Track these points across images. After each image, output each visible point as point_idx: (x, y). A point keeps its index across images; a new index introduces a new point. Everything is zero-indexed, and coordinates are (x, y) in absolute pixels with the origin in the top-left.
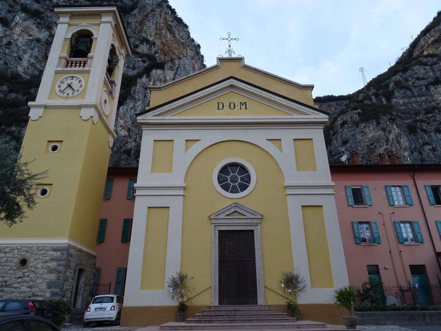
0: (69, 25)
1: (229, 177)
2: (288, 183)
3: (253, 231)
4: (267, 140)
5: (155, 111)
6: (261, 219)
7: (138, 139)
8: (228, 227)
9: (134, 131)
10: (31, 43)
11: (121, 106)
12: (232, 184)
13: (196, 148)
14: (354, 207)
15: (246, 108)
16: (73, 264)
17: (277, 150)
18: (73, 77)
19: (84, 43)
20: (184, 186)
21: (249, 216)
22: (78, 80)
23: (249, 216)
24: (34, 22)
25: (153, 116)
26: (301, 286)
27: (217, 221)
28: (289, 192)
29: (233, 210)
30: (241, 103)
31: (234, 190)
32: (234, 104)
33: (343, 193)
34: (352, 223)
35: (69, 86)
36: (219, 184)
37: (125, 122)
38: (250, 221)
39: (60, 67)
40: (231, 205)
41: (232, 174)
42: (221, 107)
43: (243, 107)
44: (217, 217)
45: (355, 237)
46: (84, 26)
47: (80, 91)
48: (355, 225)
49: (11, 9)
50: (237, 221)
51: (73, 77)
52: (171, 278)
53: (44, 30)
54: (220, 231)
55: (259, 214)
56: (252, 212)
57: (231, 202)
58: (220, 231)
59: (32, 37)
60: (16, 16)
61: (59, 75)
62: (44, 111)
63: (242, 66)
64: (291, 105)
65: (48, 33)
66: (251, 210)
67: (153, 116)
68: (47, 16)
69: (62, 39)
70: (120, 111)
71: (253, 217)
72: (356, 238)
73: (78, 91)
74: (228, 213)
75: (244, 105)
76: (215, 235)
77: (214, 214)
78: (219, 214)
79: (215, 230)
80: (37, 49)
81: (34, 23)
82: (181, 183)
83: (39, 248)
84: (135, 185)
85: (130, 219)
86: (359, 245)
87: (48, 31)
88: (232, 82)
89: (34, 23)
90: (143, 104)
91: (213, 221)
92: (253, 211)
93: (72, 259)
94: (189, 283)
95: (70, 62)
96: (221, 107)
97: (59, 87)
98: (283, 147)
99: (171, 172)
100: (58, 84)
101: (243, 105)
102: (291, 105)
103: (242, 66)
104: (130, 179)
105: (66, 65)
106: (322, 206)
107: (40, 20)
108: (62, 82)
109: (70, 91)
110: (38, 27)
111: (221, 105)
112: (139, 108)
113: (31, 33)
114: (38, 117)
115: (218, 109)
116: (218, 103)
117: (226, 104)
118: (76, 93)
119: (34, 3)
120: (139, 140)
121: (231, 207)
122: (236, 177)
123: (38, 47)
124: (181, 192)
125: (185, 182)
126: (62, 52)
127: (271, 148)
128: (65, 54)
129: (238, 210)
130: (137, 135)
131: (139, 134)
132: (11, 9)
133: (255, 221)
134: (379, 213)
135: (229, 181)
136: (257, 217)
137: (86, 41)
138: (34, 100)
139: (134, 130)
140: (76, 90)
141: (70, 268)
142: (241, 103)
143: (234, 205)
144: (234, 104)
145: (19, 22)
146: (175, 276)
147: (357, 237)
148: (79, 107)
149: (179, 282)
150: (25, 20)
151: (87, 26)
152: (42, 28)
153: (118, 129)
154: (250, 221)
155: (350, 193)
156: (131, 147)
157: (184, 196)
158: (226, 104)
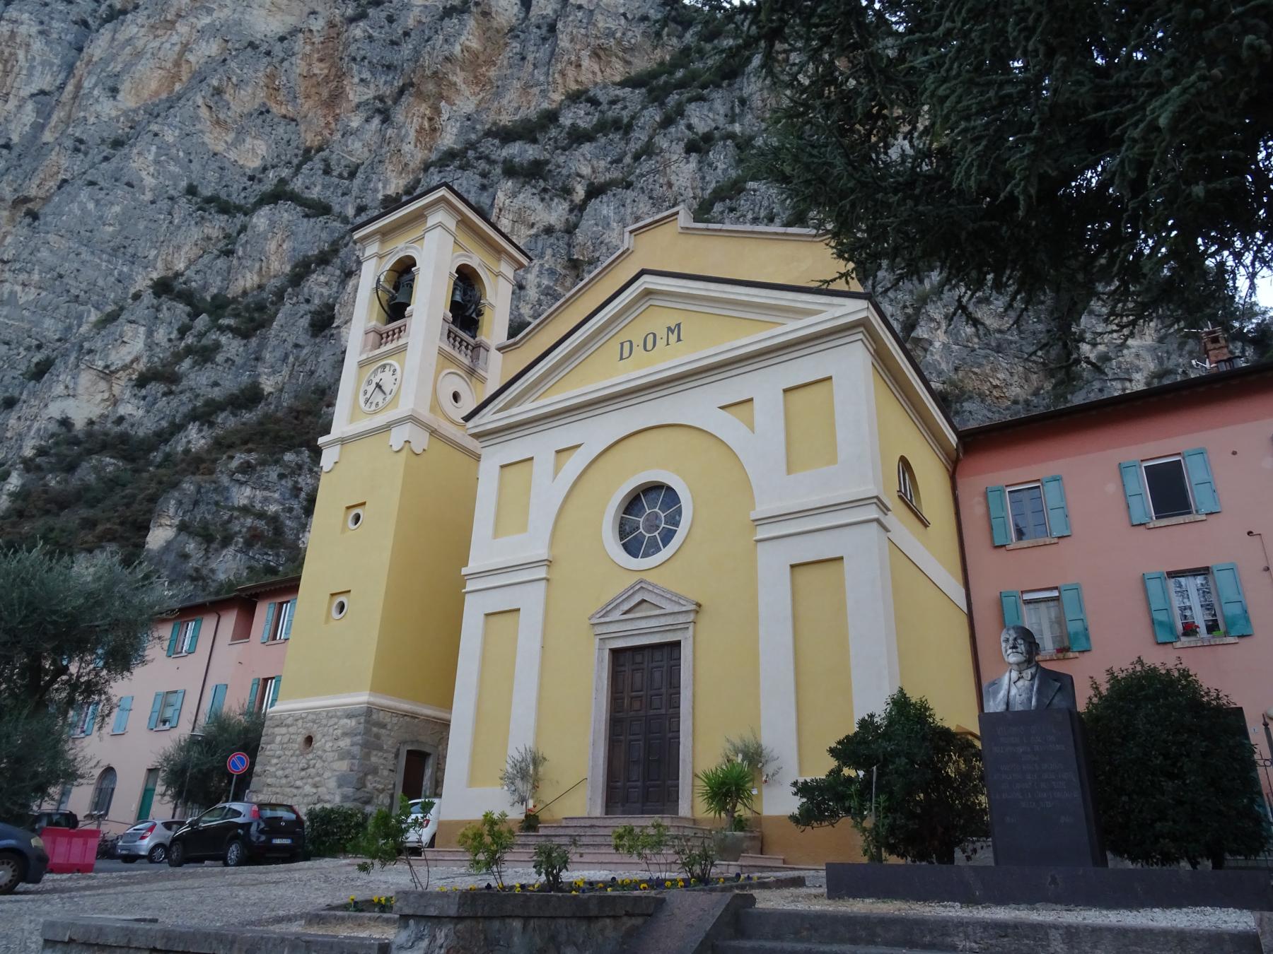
2: (763, 508)
4: (720, 408)
5: (496, 402)
8: (628, 639)
10: (536, 243)
13: (575, 464)
14: (1151, 525)
15: (679, 340)
16: (388, 743)
18: (384, 366)
21: (670, 608)
24: (534, 191)
26: (769, 769)
28: (763, 533)
29: (637, 599)
30: (669, 329)
32: (655, 336)
33: (1112, 488)
34: (1144, 580)
35: (379, 386)
38: (669, 620)
43: (673, 338)
44: (603, 620)
45: (1153, 621)
48: (1154, 586)
49: (485, 181)
50: (643, 624)
51: (384, 366)
53: (556, 200)
56: (675, 598)
58: (615, 653)
59: (536, 227)
60: (496, 193)
62: (342, 448)
63: (680, 230)
64: (776, 298)
65: (566, 205)
66: (671, 593)
68: (559, 166)
71: (677, 609)
72: (1157, 628)
74: (626, 607)
76: (601, 661)
78: (607, 612)
80: (549, 251)
81: (534, 194)
82: (542, 553)
83: (331, 714)
84: (464, 571)
86: (1170, 646)
87: (565, 199)
88: (648, 282)
89: (534, 194)
92: (676, 595)
93: (383, 731)
95: (384, 336)
98: (759, 418)
102: (776, 298)
103: (680, 230)
105: (378, 343)
106: (841, 558)
107: (545, 180)
109: (379, 397)
110: (543, 200)
113: (532, 219)
114: (332, 464)
115: (621, 359)
117: (638, 341)
118: (389, 398)
119: (527, 146)
121: (631, 592)
123: (551, 245)
124: (541, 573)
126: (369, 320)
127: (727, 427)
132: (485, 181)
133: (682, 619)
134: (1250, 533)
136: (684, 609)
141: (380, 748)
142: (669, 329)
143: (638, 587)
145: (504, 204)
147: (1161, 623)
148: (388, 427)
150: (514, 195)
151: (407, 248)
152: (552, 199)
154: (669, 620)
155: (1140, 485)
157: (548, 580)
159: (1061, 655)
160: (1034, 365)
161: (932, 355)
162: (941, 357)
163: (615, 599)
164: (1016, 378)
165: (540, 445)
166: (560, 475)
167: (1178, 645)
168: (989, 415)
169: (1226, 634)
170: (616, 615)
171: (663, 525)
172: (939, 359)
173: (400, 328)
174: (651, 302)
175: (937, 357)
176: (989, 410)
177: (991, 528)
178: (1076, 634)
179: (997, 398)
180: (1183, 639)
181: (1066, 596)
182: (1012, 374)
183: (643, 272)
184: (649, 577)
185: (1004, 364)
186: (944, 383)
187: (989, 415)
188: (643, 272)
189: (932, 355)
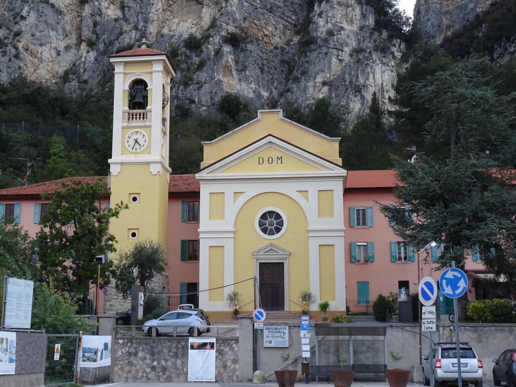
0: (125, 74)
1: (267, 222)
2: (310, 228)
3: (283, 263)
5: (208, 169)
6: (289, 255)
7: (141, 24)
9: (133, 8)
12: (270, 227)
13: (242, 199)
15: (282, 163)
17: (305, 201)
18: (137, 132)
19: (140, 91)
20: (234, 230)
21: (281, 253)
22: (142, 135)
23: (281, 253)
25: (207, 173)
26: (313, 299)
27: (258, 257)
28: (311, 234)
29: (269, 248)
30: (278, 157)
31: (271, 233)
34: (391, 243)
35: (136, 141)
36: (260, 227)
38: (281, 256)
39: (125, 122)
40: (268, 245)
41: (269, 220)
42: (261, 162)
43: (279, 161)
44: (258, 254)
45: (391, 256)
46: (138, 75)
47: (145, 146)
48: (393, 245)
50: (272, 256)
52: (228, 294)
54: (260, 263)
55: (287, 251)
56: (283, 250)
57: (268, 242)
58: (260, 263)
61: (126, 130)
67: (207, 173)
69: (122, 92)
71: (284, 253)
73: (144, 146)
74: (265, 250)
75: (280, 159)
76: (257, 266)
77: (256, 251)
79: (256, 262)
82: (232, 228)
85: (186, 240)
88: (270, 139)
91: (255, 257)
92: (284, 249)
94: (239, 298)
95: (131, 114)
96: (261, 162)
97: (128, 142)
98: (310, 198)
99: (224, 219)
100: (126, 139)
101: (279, 159)
104: (182, 202)
108: (129, 137)
109: (137, 146)
111: (261, 160)
115: (259, 164)
116: (259, 158)
117: (266, 159)
118: (143, 148)
120: (143, 26)
122: (273, 222)
124: (232, 235)
125: (234, 227)
126: (123, 106)
127: (300, 199)
128: (127, 108)
129: (273, 248)
130: (138, 15)
131: (142, 13)
133: (285, 256)
135: (267, 225)
136: (286, 254)
137: (141, 89)
139: (132, 6)
140: (142, 145)
142: (278, 157)
146: (231, 293)
147: (393, 256)
148: (148, 163)
149: (233, 297)
151: (141, 75)
153: (103, 4)
154: (281, 256)
156: (130, 41)
158: (266, 159)
159: (365, 263)
160: (289, 25)
161: (231, 6)
162: (237, 9)
163: (262, 248)
164: (278, 31)
165: (229, 189)
166: (237, 201)
167: (397, 263)
168: (261, 54)
169: (409, 261)
170: (262, 253)
172: (235, 10)
174: (270, 145)
175: (234, 8)
176: (261, 51)
177: (350, 221)
178: (371, 257)
179: (266, 43)
181: (369, 245)
182: (276, 28)
183: (270, 135)
184: (274, 242)
185: (272, 21)
186: (236, 27)
187: (261, 54)
188: (270, 135)
189: (231, 6)
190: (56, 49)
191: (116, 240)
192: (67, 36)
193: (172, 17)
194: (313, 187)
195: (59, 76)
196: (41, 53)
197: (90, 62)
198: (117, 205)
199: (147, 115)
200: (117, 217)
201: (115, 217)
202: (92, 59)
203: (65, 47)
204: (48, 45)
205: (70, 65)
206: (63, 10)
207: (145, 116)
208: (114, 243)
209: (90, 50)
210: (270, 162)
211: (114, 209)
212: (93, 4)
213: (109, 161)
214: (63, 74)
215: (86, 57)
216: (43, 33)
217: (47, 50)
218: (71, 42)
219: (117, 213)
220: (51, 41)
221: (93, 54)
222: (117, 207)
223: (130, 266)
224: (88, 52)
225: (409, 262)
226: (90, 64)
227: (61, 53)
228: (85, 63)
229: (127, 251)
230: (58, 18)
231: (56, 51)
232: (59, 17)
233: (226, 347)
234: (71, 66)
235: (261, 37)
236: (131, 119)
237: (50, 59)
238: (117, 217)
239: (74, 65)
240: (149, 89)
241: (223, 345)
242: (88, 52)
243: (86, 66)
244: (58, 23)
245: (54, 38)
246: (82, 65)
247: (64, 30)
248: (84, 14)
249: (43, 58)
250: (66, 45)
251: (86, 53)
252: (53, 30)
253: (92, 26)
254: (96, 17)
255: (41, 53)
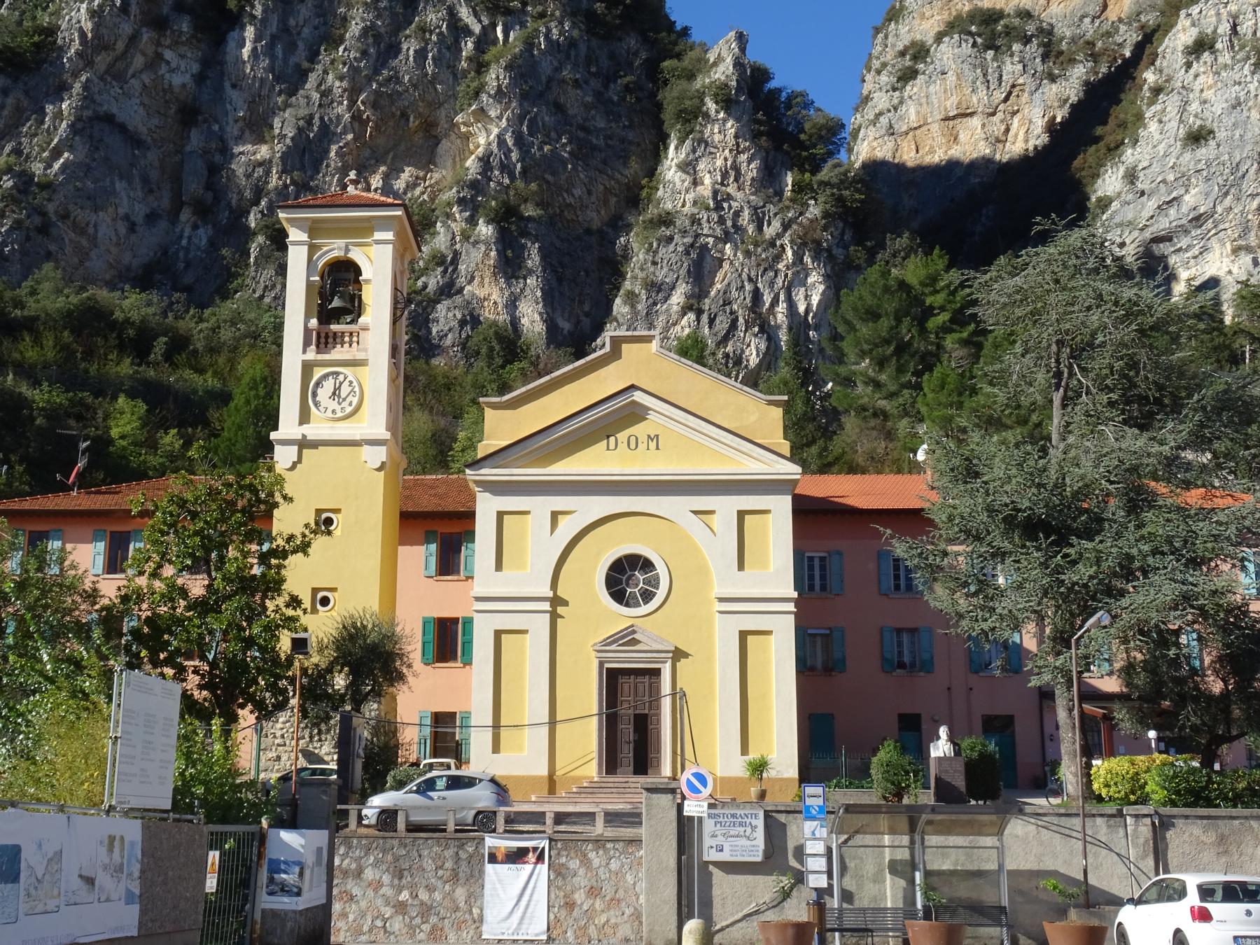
4: (692, 511)
11: (233, 30)
13: (568, 528)
15: (657, 448)
18: (337, 374)
30: (649, 436)
32: (637, 438)
33: (872, 566)
34: (882, 630)
37: (254, 101)
43: (653, 445)
45: (883, 658)
70: (228, 49)
90: (318, 16)
101: (652, 440)
112: (303, 35)
115: (608, 449)
138: (276, 428)
142: (649, 436)
144: (637, 438)
153: (229, 129)
160: (616, 186)
164: (593, 199)
165: (542, 506)
167: (894, 674)
168: (558, 244)
169: (920, 671)
170: (613, 647)
171: (641, 585)
173: (343, 333)
176: (558, 237)
179: (568, 221)
180: (898, 671)
182: (589, 192)
183: (633, 387)
185: (582, 176)
187: (558, 244)
190: (127, 217)
191: (303, 606)
192: (151, 191)
193: (373, 162)
194: (727, 506)
195: (133, 274)
196: (95, 226)
197: (199, 248)
198: (307, 526)
199: (358, 336)
200: (306, 554)
201: (300, 555)
202: (204, 241)
203: (147, 216)
204: (110, 210)
205: (156, 253)
206: (144, 137)
207: (355, 339)
208: (299, 612)
209: (199, 223)
210: (633, 445)
211: (299, 536)
212: (209, 127)
213: (273, 436)
214: (140, 272)
215: (190, 238)
216: (101, 184)
217: (109, 220)
218: (159, 206)
219: (308, 545)
220: (117, 201)
221: (206, 233)
222: (307, 532)
223: (329, 670)
224: (195, 227)
225: (922, 674)
226: (199, 253)
227: (137, 228)
228: (187, 250)
229: (321, 635)
230: (134, 154)
231: (126, 223)
232: (136, 152)
233: (571, 858)
234: (159, 254)
235: (559, 207)
236: (322, 346)
237: (114, 239)
238: (306, 554)
239: (165, 253)
240: (364, 280)
241: (564, 853)
242: (195, 227)
243: (190, 256)
244: (132, 165)
245: (123, 194)
246: (181, 254)
247: (145, 180)
248: (188, 148)
249: (100, 235)
250: (148, 212)
251: (190, 229)
252: (121, 178)
253: (206, 173)
254: (213, 157)
255: (95, 226)
